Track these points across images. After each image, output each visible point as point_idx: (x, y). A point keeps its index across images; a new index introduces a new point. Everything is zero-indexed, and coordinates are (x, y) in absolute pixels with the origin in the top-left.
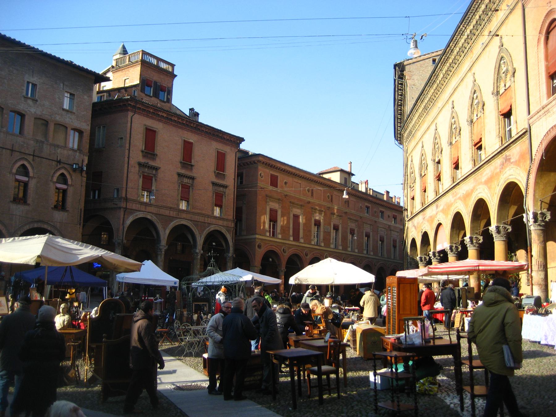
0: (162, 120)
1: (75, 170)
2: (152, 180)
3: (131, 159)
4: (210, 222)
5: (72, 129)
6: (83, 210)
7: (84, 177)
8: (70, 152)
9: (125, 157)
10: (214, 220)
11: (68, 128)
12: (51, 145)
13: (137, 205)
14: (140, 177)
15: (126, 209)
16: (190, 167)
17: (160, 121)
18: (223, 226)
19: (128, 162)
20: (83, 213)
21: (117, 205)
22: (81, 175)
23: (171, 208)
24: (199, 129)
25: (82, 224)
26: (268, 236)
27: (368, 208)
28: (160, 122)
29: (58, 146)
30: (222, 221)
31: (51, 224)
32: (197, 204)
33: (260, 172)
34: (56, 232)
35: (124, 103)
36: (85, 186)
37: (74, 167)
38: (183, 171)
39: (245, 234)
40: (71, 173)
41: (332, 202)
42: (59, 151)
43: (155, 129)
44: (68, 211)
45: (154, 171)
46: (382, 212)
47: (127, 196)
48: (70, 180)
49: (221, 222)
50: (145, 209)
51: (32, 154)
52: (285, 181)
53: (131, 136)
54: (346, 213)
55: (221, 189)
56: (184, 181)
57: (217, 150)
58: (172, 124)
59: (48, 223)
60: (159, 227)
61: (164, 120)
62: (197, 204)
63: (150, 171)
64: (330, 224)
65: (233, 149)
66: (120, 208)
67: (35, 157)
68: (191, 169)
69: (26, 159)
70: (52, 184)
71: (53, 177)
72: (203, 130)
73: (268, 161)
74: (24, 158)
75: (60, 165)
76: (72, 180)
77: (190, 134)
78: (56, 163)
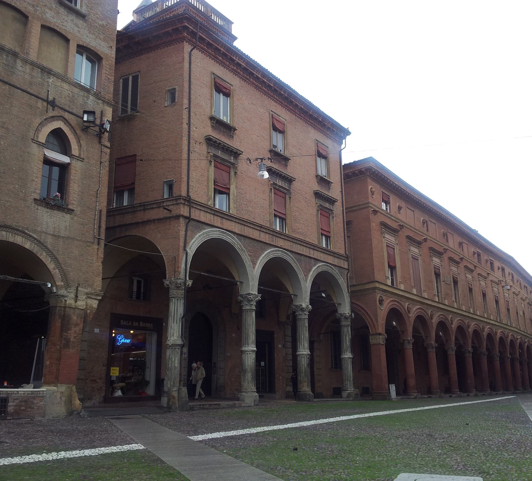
1: (86, 128)
3: (193, 128)
4: (317, 258)
6: (104, 213)
7: (106, 147)
8: (76, 90)
9: (182, 123)
10: (322, 255)
12: (33, 64)
14: (210, 164)
15: (189, 219)
16: (283, 162)
17: (235, 73)
19: (189, 132)
20: (104, 218)
21: (171, 211)
22: (100, 142)
23: (261, 226)
25: (102, 243)
26: (389, 286)
31: (31, 236)
32: (297, 225)
33: (370, 187)
34: (44, 254)
35: (174, 27)
36: (107, 164)
37: (85, 118)
40: (78, 132)
41: (447, 242)
44: (73, 210)
47: (190, 194)
48: (77, 147)
49: (330, 259)
50: (222, 223)
52: (397, 205)
54: (462, 259)
55: (327, 205)
57: (316, 141)
58: (253, 83)
59: (24, 233)
60: (246, 257)
63: (226, 157)
65: (336, 145)
66: (178, 217)
70: (34, 146)
76: (80, 146)
78: (45, 104)
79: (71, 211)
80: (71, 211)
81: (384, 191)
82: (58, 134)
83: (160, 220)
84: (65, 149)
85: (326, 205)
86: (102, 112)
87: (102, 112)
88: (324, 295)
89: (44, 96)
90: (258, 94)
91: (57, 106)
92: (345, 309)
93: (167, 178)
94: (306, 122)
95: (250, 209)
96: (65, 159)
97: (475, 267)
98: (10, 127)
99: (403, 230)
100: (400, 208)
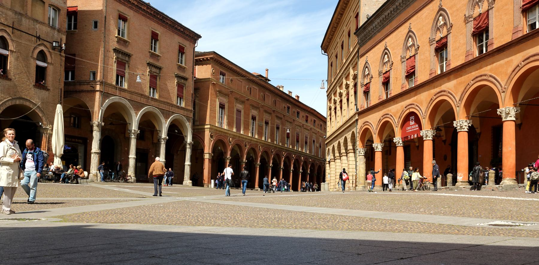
0: (133, 8)
2: (125, 66)
5: (50, 5)
7: (63, 57)
10: (177, 109)
11: (46, 3)
13: (113, 90)
18: (184, 116)
21: (94, 87)
24: (165, 21)
27: (288, 108)
28: (131, 9)
29: (37, 21)
30: (183, 111)
32: (163, 93)
36: (64, 66)
37: (54, 45)
38: (151, 61)
39: (198, 124)
42: (38, 26)
43: (127, 16)
44: (49, 89)
45: (127, 58)
46: (298, 113)
48: (50, 59)
50: (120, 94)
51: (11, 26)
53: (106, 20)
54: (274, 111)
56: (153, 71)
58: (141, 13)
61: (135, 8)
62: (163, 93)
64: (262, 120)
65: (191, 44)
67: (14, 30)
68: (158, 60)
69: (4, 30)
70: (32, 60)
71: (33, 52)
72: (168, 23)
73: (219, 59)
74: (3, 29)
75: (39, 41)
76: (52, 58)
77: (156, 25)
78: (36, 38)
79: (48, 90)
80: (48, 90)
81: (222, 70)
82: (42, 53)
83: (88, 91)
84: (44, 60)
85: (182, 81)
86: (61, 39)
87: (61, 39)
88: (176, 131)
89: (35, 34)
90: (143, 18)
91: (41, 39)
92: (189, 139)
93: (92, 70)
94: (173, 32)
95: (136, 85)
96: (44, 65)
97: (284, 116)
98: (22, 52)
99: (233, 94)
100: (231, 80)
